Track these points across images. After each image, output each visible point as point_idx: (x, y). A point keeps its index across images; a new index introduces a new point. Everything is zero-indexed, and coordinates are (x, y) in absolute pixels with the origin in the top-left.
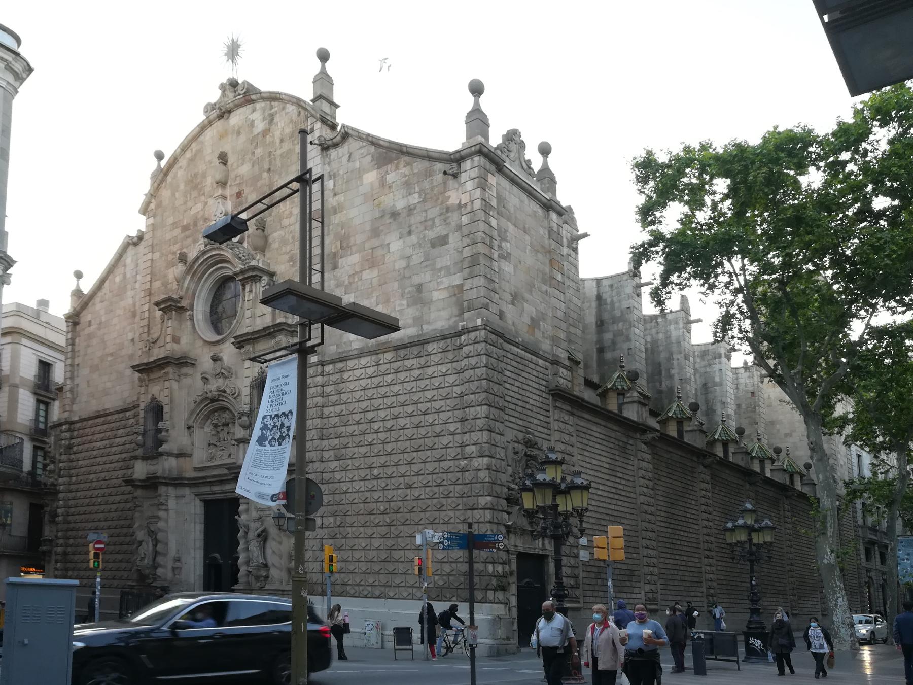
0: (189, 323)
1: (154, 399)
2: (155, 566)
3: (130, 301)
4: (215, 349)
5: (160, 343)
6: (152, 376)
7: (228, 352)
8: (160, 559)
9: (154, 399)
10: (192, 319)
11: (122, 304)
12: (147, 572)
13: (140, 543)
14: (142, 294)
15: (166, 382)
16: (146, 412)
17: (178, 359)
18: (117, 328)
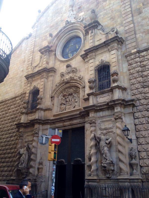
0: (54, 56)
1: (35, 87)
2: (28, 167)
3: (23, 57)
4: (69, 63)
5: (40, 65)
6: (34, 79)
7: (77, 62)
8: (32, 163)
9: (35, 87)
10: (55, 55)
11: (19, 59)
12: (24, 171)
13: (21, 155)
14: (29, 53)
15: (42, 80)
16: (30, 93)
17: (49, 69)
18: (16, 68)
